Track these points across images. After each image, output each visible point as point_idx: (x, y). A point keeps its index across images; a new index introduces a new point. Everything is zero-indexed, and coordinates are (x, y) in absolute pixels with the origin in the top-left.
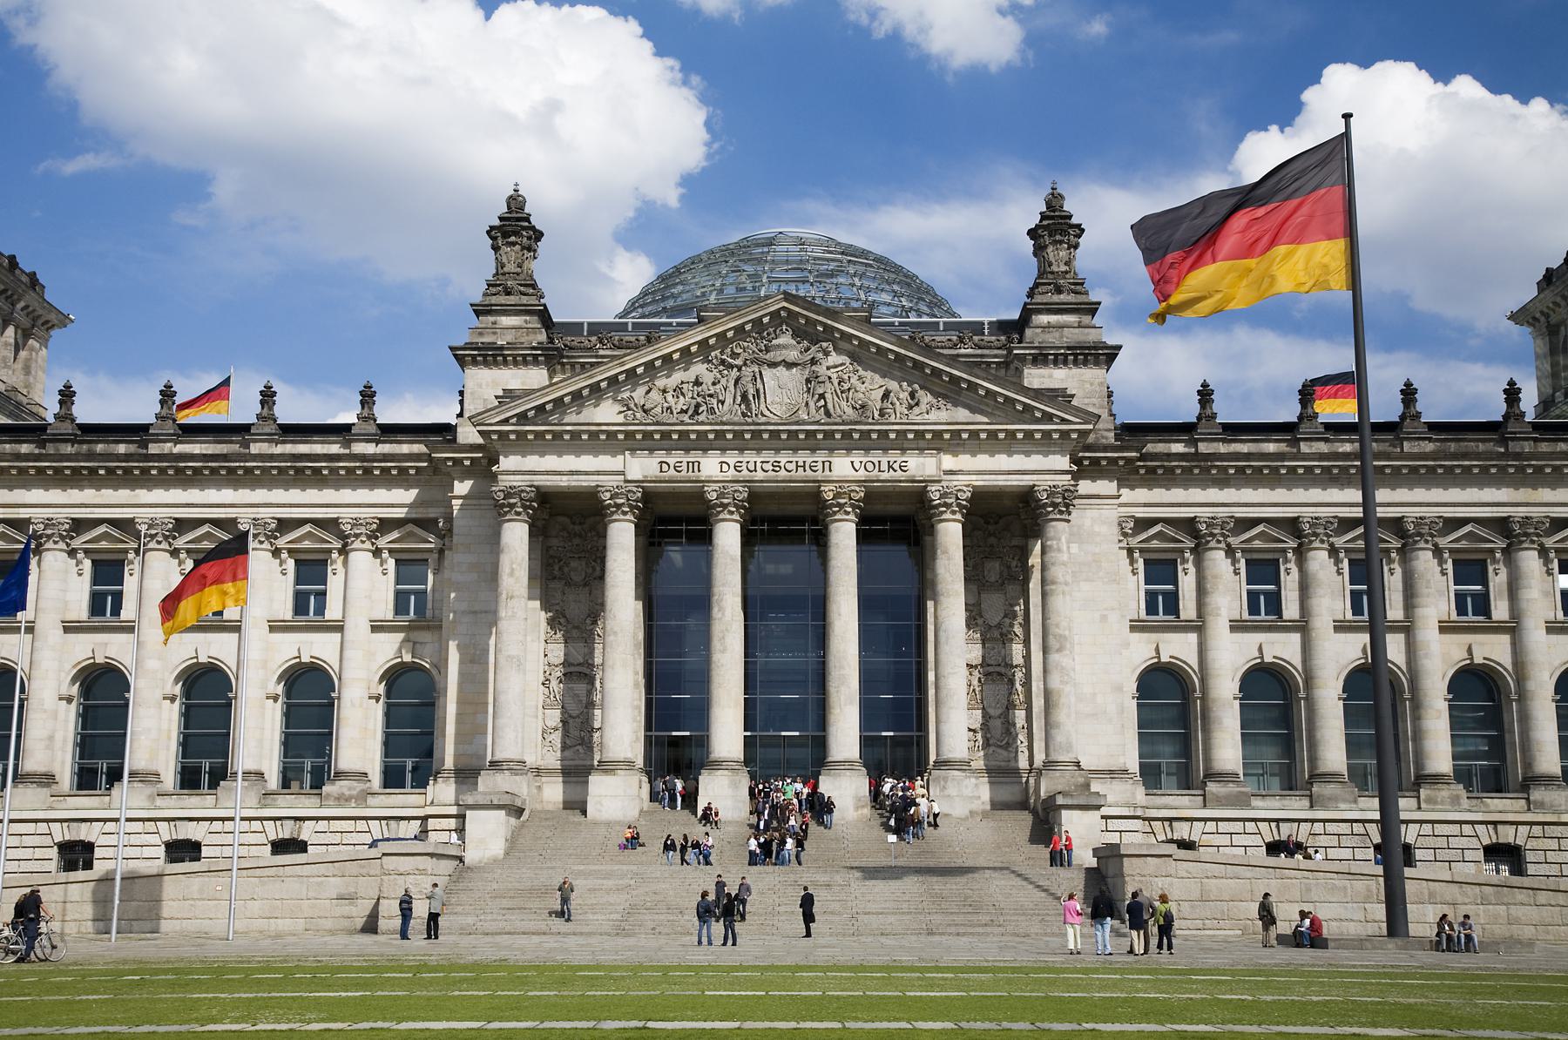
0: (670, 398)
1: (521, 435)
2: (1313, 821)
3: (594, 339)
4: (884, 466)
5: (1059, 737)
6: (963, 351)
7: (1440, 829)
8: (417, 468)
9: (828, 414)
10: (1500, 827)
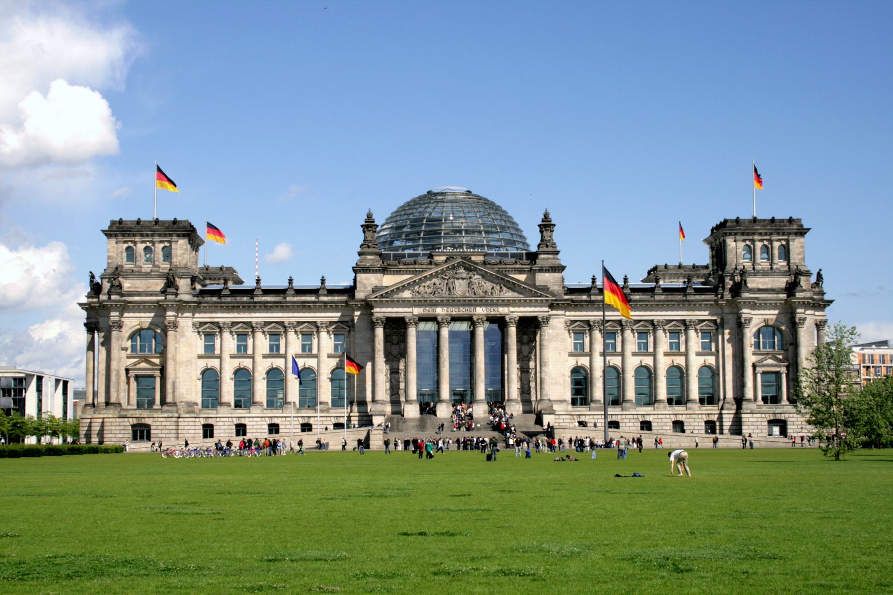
0: (426, 289)
1: (382, 301)
2: (622, 415)
3: (397, 262)
4: (492, 309)
5: (544, 392)
6: (518, 266)
7: (660, 416)
8: (342, 306)
9: (475, 294)
10: (677, 416)
